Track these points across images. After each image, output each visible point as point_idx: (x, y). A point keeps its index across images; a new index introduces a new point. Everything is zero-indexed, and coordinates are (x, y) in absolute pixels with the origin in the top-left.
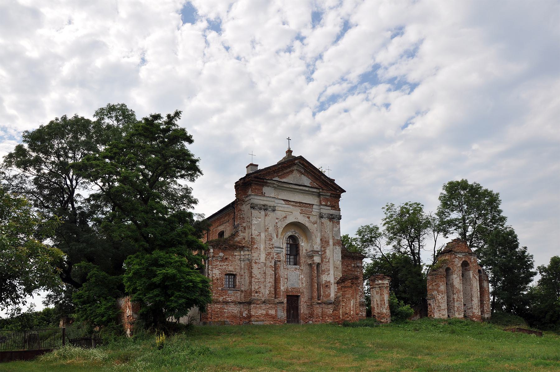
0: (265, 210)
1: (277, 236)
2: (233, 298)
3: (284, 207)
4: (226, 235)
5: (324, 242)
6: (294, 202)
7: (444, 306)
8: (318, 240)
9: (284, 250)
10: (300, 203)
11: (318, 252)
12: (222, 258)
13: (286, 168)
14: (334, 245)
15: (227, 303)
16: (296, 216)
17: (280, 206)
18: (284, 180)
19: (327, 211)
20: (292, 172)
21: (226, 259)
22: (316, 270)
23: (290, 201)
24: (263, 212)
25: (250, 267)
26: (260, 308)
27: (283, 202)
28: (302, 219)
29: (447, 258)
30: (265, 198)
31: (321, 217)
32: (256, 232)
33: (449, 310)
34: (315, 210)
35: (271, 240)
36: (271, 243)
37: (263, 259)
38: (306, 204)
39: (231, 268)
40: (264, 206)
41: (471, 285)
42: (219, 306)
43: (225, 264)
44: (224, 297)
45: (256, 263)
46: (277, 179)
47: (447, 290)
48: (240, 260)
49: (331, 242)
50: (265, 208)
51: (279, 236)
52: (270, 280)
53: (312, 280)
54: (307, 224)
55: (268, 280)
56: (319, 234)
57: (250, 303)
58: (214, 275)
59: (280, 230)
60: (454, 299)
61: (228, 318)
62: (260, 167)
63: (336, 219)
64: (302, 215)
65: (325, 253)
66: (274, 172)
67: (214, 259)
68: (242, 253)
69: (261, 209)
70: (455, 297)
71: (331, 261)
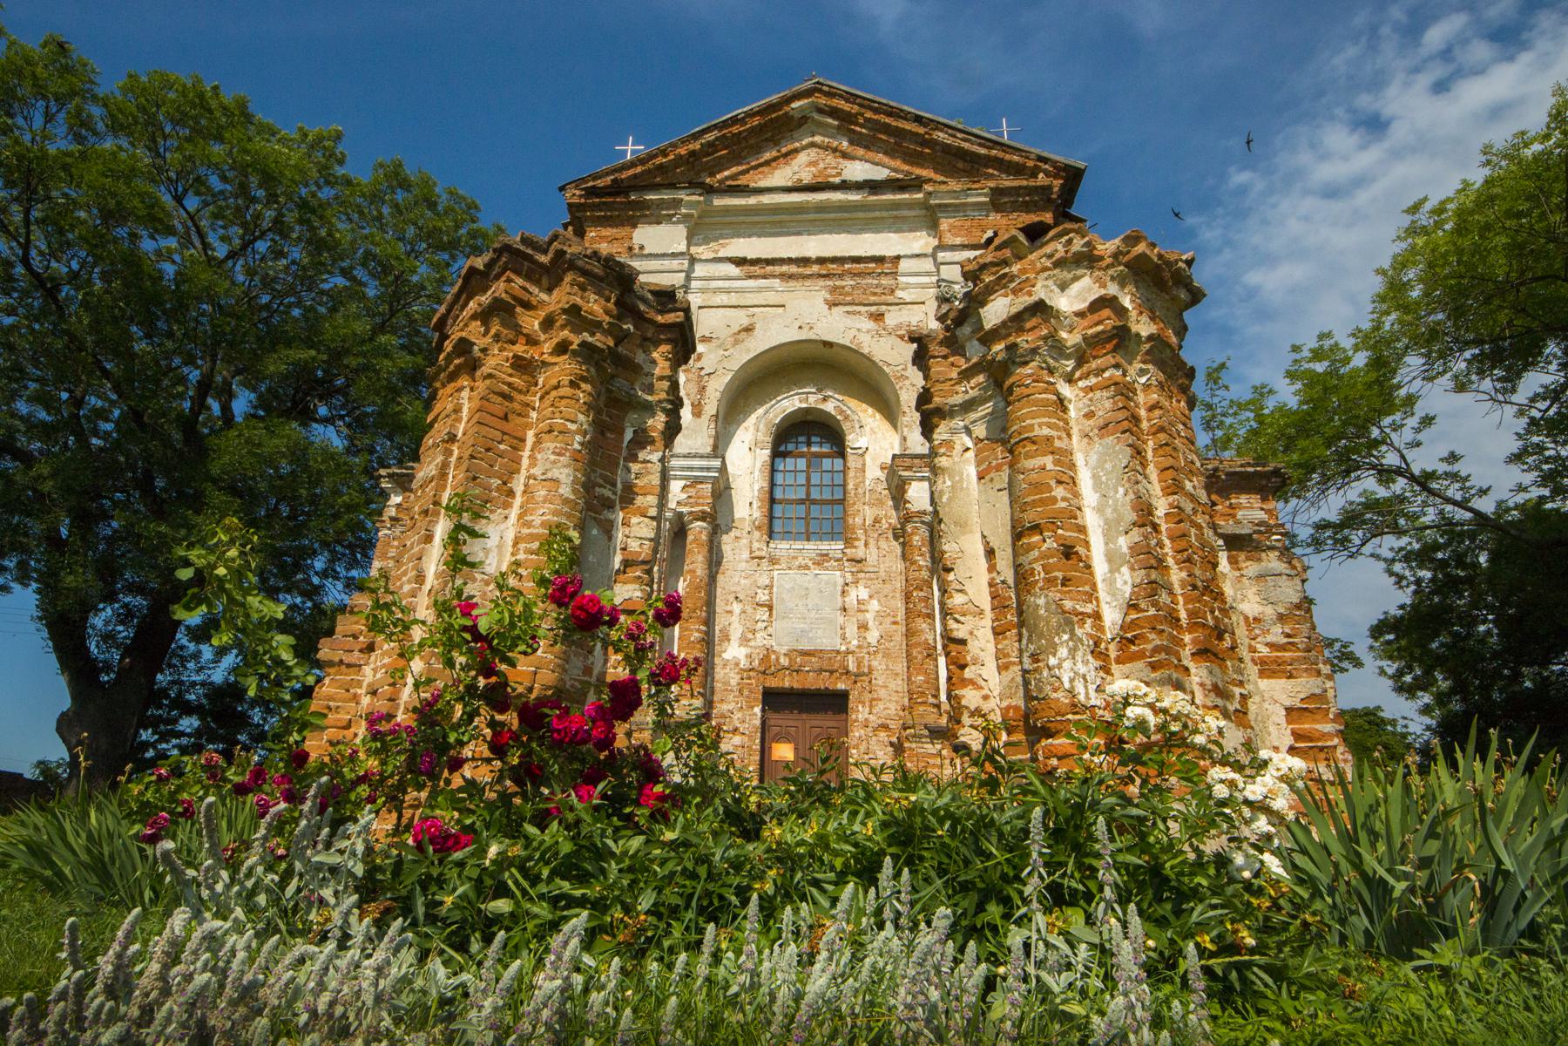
6: (790, 261)
10: (821, 261)
16: (807, 315)
23: (770, 262)
27: (733, 270)
38: (857, 260)
64: (835, 310)
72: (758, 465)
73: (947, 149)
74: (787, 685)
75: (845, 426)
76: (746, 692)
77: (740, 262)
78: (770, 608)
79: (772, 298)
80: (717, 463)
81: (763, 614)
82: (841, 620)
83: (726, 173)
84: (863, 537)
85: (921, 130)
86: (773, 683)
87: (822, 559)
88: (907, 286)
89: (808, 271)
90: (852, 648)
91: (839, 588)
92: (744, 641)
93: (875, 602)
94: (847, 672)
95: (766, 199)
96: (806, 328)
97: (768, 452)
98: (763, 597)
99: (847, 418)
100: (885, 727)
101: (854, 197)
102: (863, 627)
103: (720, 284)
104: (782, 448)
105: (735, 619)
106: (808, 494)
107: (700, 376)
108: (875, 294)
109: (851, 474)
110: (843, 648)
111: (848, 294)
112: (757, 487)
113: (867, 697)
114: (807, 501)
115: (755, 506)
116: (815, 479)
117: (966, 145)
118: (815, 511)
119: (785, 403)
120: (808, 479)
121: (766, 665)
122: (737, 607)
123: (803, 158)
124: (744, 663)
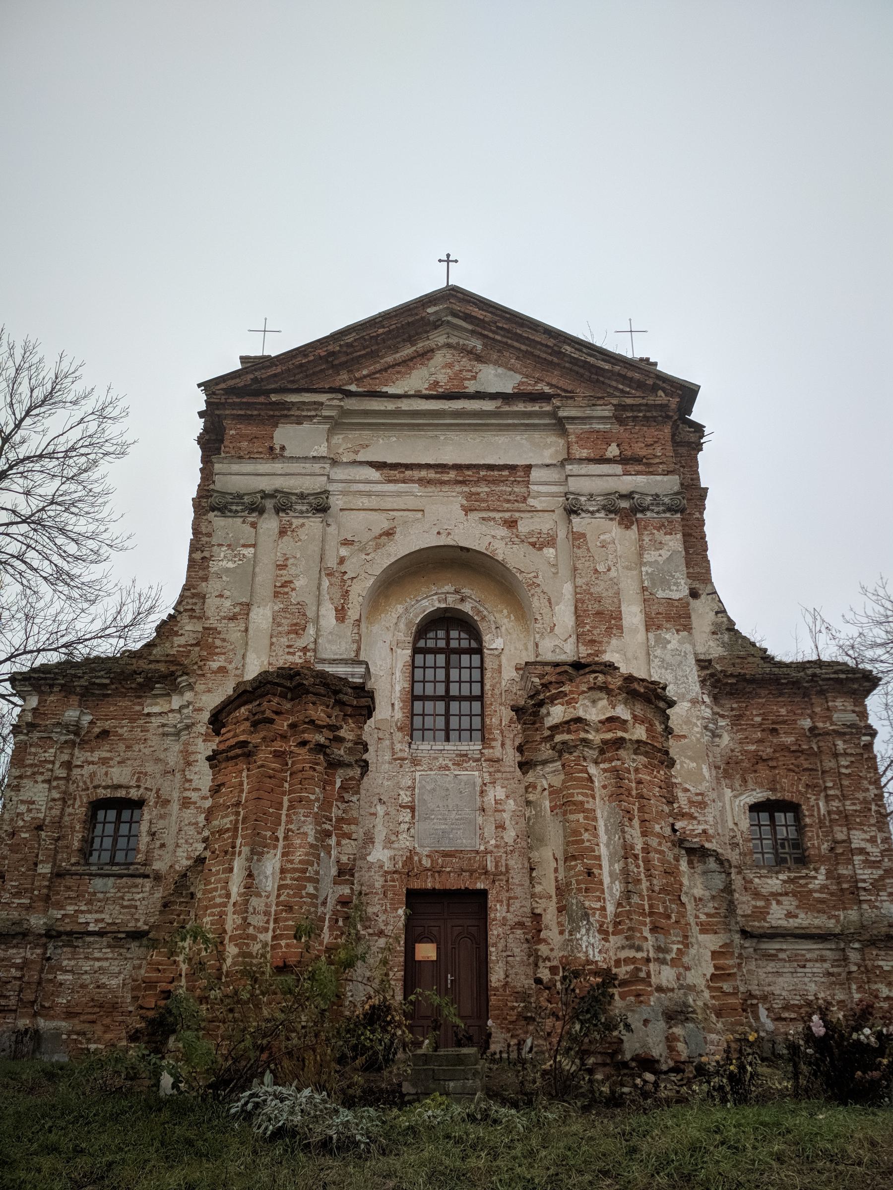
0: (278, 510)
1: (341, 614)
2: (111, 915)
3: (379, 494)
6: (428, 466)
8: (564, 616)
10: (458, 467)
14: (651, 624)
17: (361, 493)
20: (426, 355)
21: (105, 734)
27: (374, 474)
30: (278, 467)
32: (228, 603)
34: (544, 490)
35: (297, 630)
36: (301, 643)
38: (490, 467)
39: (120, 774)
43: (96, 756)
44: (70, 909)
49: (633, 615)
50: (282, 503)
51: (353, 614)
56: (567, 589)
58: (23, 808)
59: (360, 589)
61: (69, 1015)
66: (337, 368)
67: (36, 735)
68: (176, 702)
72: (400, 665)
73: (574, 361)
74: (429, 886)
75: (482, 626)
76: (390, 895)
77: (379, 466)
78: (413, 809)
79: (411, 502)
80: (361, 670)
81: (406, 816)
82: (480, 820)
83: (365, 372)
84: (500, 738)
85: (551, 342)
86: (416, 885)
87: (462, 758)
88: (539, 494)
89: (445, 477)
90: (490, 848)
91: (478, 789)
92: (388, 843)
93: (511, 802)
94: (486, 873)
95: (405, 405)
96: (443, 536)
97: (409, 652)
98: (405, 798)
99: (483, 618)
100: (521, 924)
101: (488, 406)
102: (501, 827)
103: (361, 487)
104: (421, 644)
105: (379, 821)
106: (447, 690)
107: (343, 581)
108: (508, 501)
109: (488, 674)
110: (482, 848)
111: (484, 501)
112: (398, 688)
113: (504, 895)
114: (447, 698)
115: (396, 707)
116: (454, 674)
117: (590, 359)
118: (454, 706)
119: (425, 603)
120: (447, 675)
121: (409, 866)
122: (380, 810)
123: (439, 358)
124: (388, 866)
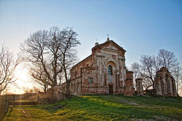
2: (92, 86)
4: (89, 66)
5: (120, 67)
7: (160, 89)
8: (118, 67)
9: (107, 70)
11: (118, 71)
12: (88, 72)
13: (107, 44)
14: (123, 68)
15: (89, 87)
18: (107, 48)
19: (121, 57)
20: (109, 45)
22: (118, 77)
24: (101, 58)
25: (97, 76)
26: (100, 89)
28: (113, 60)
29: (160, 73)
31: (119, 59)
33: (162, 91)
34: (117, 57)
35: (103, 67)
37: (101, 73)
39: (91, 76)
40: (101, 56)
41: (169, 82)
42: (87, 88)
45: (99, 74)
46: (104, 47)
47: (161, 84)
48: (94, 73)
49: (122, 68)
50: (101, 56)
52: (103, 80)
53: (117, 80)
54: (115, 62)
55: (103, 80)
57: (97, 87)
59: (106, 64)
60: (164, 87)
62: (99, 44)
63: (124, 60)
65: (121, 71)
69: (100, 57)
70: (164, 86)
71: (123, 74)
95: (109, 50)
101: (114, 50)
